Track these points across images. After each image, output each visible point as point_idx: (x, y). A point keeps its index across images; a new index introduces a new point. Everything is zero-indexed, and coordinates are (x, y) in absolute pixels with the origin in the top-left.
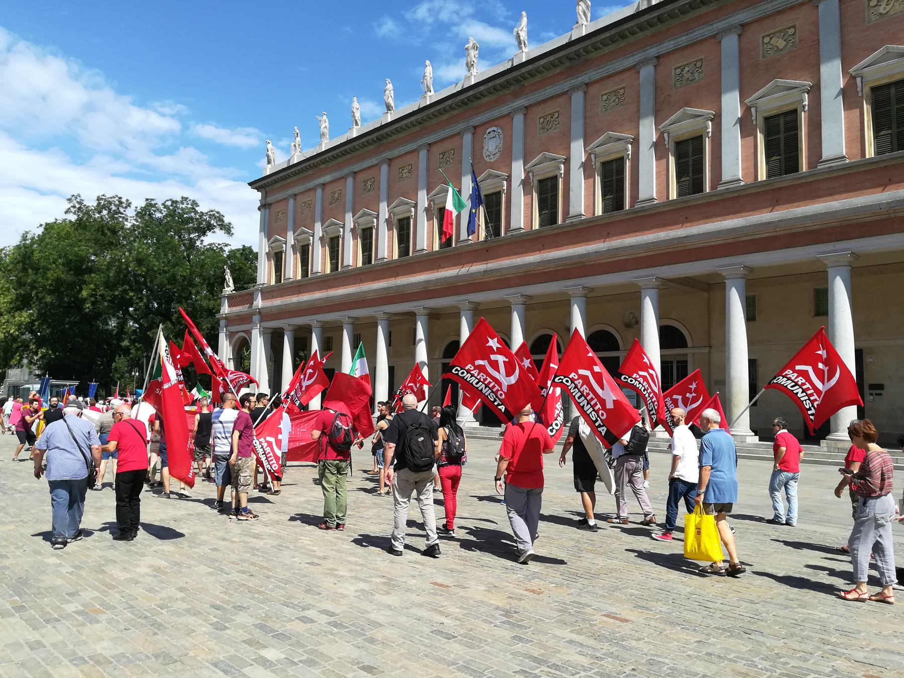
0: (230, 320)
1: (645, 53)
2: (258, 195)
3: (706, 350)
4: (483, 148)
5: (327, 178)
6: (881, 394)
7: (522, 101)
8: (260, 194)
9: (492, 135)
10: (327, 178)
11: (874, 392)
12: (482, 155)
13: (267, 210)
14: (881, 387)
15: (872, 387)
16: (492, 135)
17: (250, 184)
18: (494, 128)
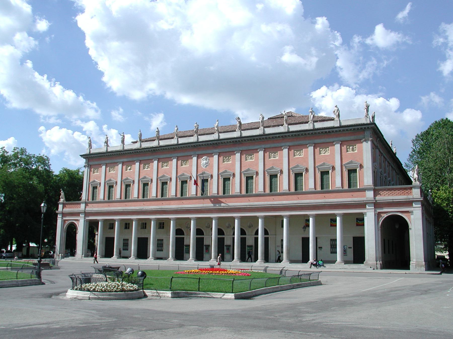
0: (64, 215)
1: (261, 146)
2: (84, 160)
3: (275, 236)
4: (201, 163)
5: (125, 160)
6: (321, 250)
7: (218, 150)
8: (85, 160)
9: (205, 159)
10: (125, 160)
11: (320, 249)
12: (201, 164)
13: (89, 168)
14: (321, 248)
15: (319, 248)
16: (205, 159)
17: (80, 155)
18: (206, 157)
